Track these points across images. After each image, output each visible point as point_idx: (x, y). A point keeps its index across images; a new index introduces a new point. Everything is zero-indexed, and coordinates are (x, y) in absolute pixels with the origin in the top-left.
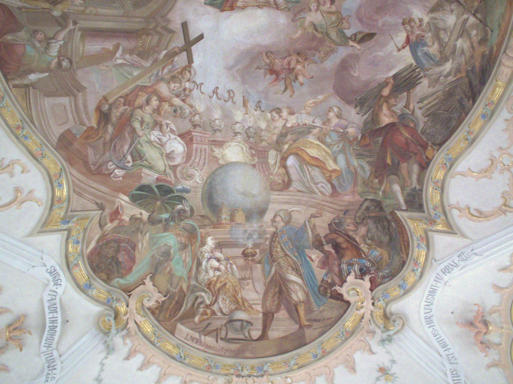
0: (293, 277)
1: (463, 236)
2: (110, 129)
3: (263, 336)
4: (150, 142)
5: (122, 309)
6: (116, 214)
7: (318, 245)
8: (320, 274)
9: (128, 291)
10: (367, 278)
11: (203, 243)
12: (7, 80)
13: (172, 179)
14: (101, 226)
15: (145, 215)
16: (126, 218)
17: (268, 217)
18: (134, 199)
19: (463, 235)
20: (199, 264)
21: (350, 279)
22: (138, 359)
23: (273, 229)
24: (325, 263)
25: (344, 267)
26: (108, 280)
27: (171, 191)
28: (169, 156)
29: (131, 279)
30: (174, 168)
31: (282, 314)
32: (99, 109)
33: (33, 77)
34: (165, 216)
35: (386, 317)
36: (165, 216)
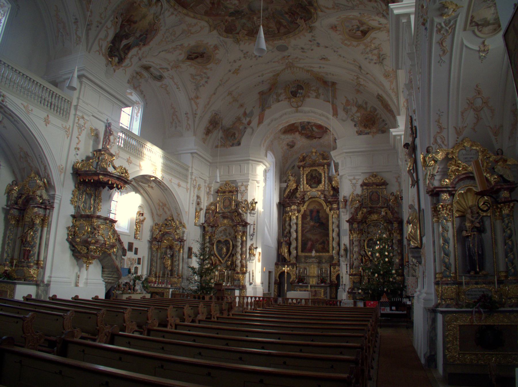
0: (282, 21)
1: (325, 12)
2: (216, 5)
3: (279, 32)
4: (228, 4)
5: (238, 37)
6: (226, 21)
7: (287, 13)
8: (290, 19)
9: (238, 33)
10: (303, 19)
11: (253, 19)
12: (186, 9)
13: (238, 9)
14: (224, 24)
15: (234, 18)
16: (230, 21)
17: (269, 10)
18: (230, 16)
19: (325, 12)
20: (254, 23)
21: (298, 19)
22: (248, 43)
23: (272, 12)
24: (290, 16)
25: (296, 17)
26: (231, 33)
27: (239, 11)
28: (234, 5)
29: (237, 31)
30: (237, 6)
31: (282, 28)
32: (211, 3)
33: (191, 5)
34: (240, 17)
35: (310, 27)
36: (240, 17)
